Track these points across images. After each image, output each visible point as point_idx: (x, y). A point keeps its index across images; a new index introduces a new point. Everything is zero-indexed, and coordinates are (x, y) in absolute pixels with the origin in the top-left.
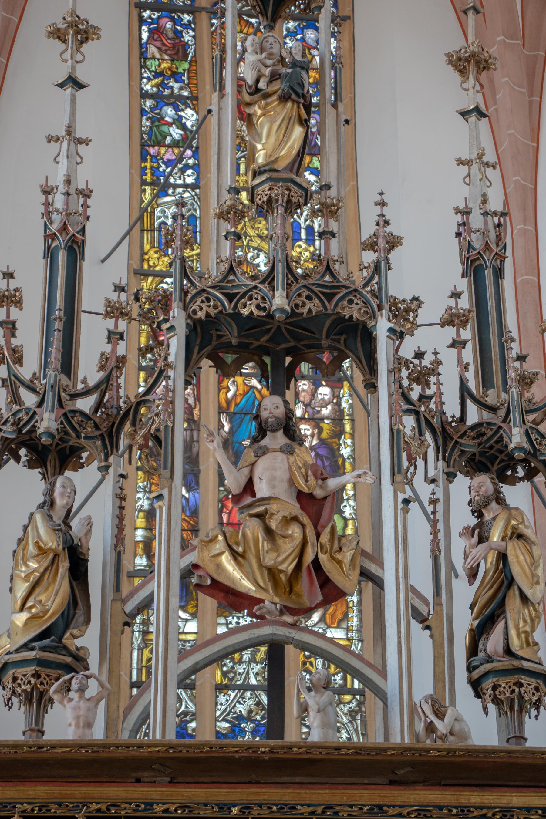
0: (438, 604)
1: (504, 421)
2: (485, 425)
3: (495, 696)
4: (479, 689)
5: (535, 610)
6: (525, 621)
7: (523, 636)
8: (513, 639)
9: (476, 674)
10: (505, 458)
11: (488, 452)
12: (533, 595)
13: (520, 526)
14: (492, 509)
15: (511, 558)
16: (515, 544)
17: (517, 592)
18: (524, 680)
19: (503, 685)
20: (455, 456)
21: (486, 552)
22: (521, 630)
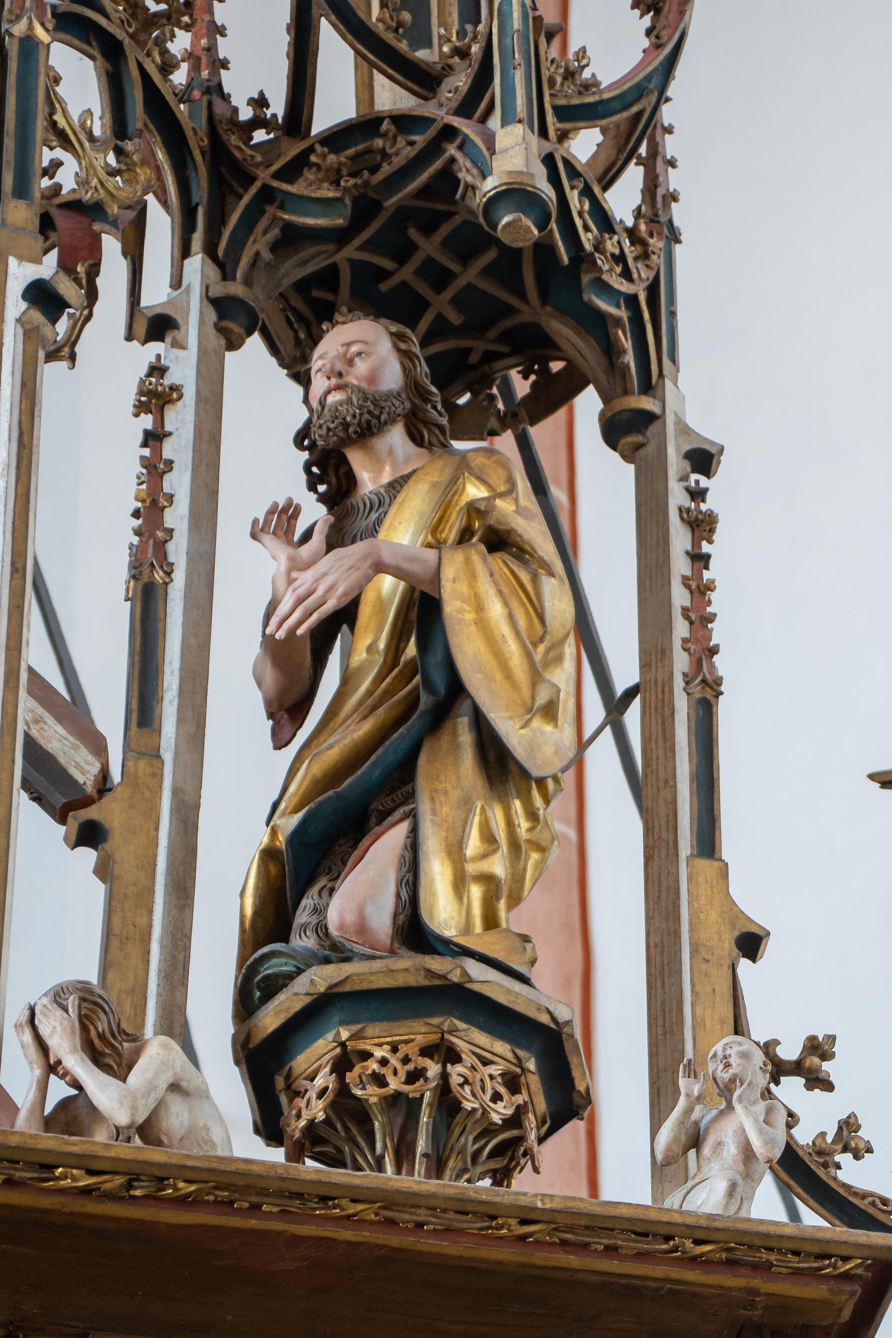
0: (141, 754)
1: (466, 108)
2: (386, 125)
3: (343, 1090)
4: (280, 1082)
5: (532, 815)
6: (489, 838)
7: (476, 892)
8: (434, 894)
9: (270, 1018)
10: (455, 318)
11: (385, 274)
12: (532, 748)
13: (498, 502)
14: (391, 452)
15: (453, 606)
16: (476, 558)
17: (466, 738)
18: (470, 1038)
19: (379, 1053)
20: (259, 244)
21: (356, 575)
22: (471, 868)
